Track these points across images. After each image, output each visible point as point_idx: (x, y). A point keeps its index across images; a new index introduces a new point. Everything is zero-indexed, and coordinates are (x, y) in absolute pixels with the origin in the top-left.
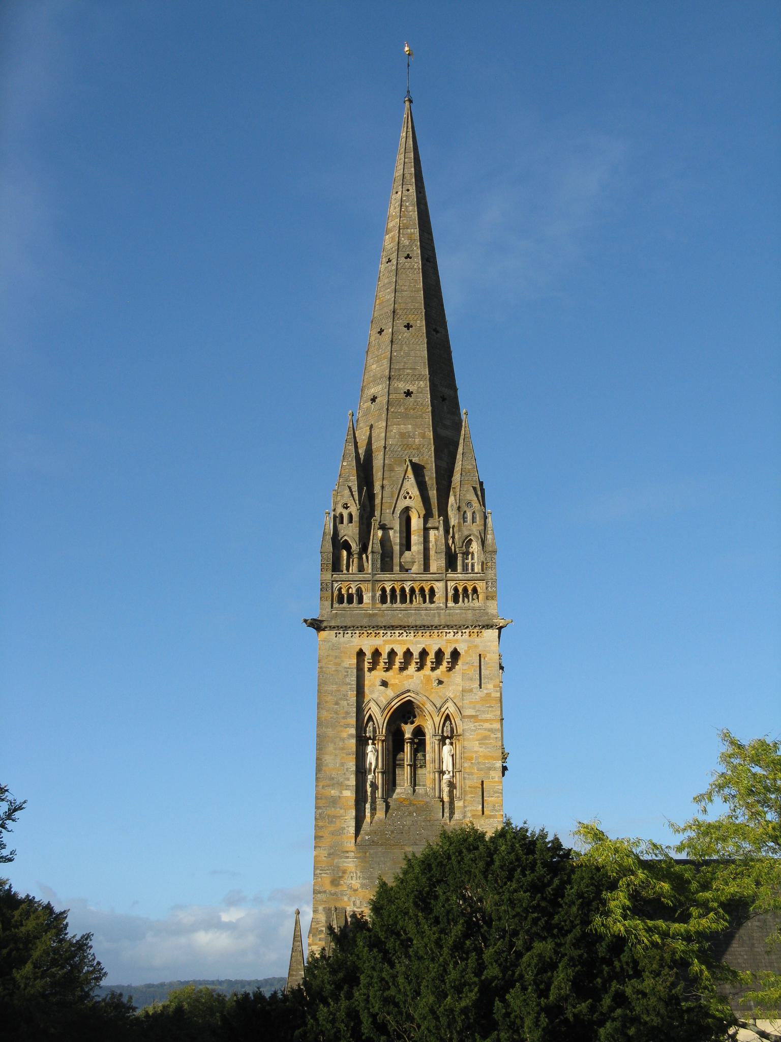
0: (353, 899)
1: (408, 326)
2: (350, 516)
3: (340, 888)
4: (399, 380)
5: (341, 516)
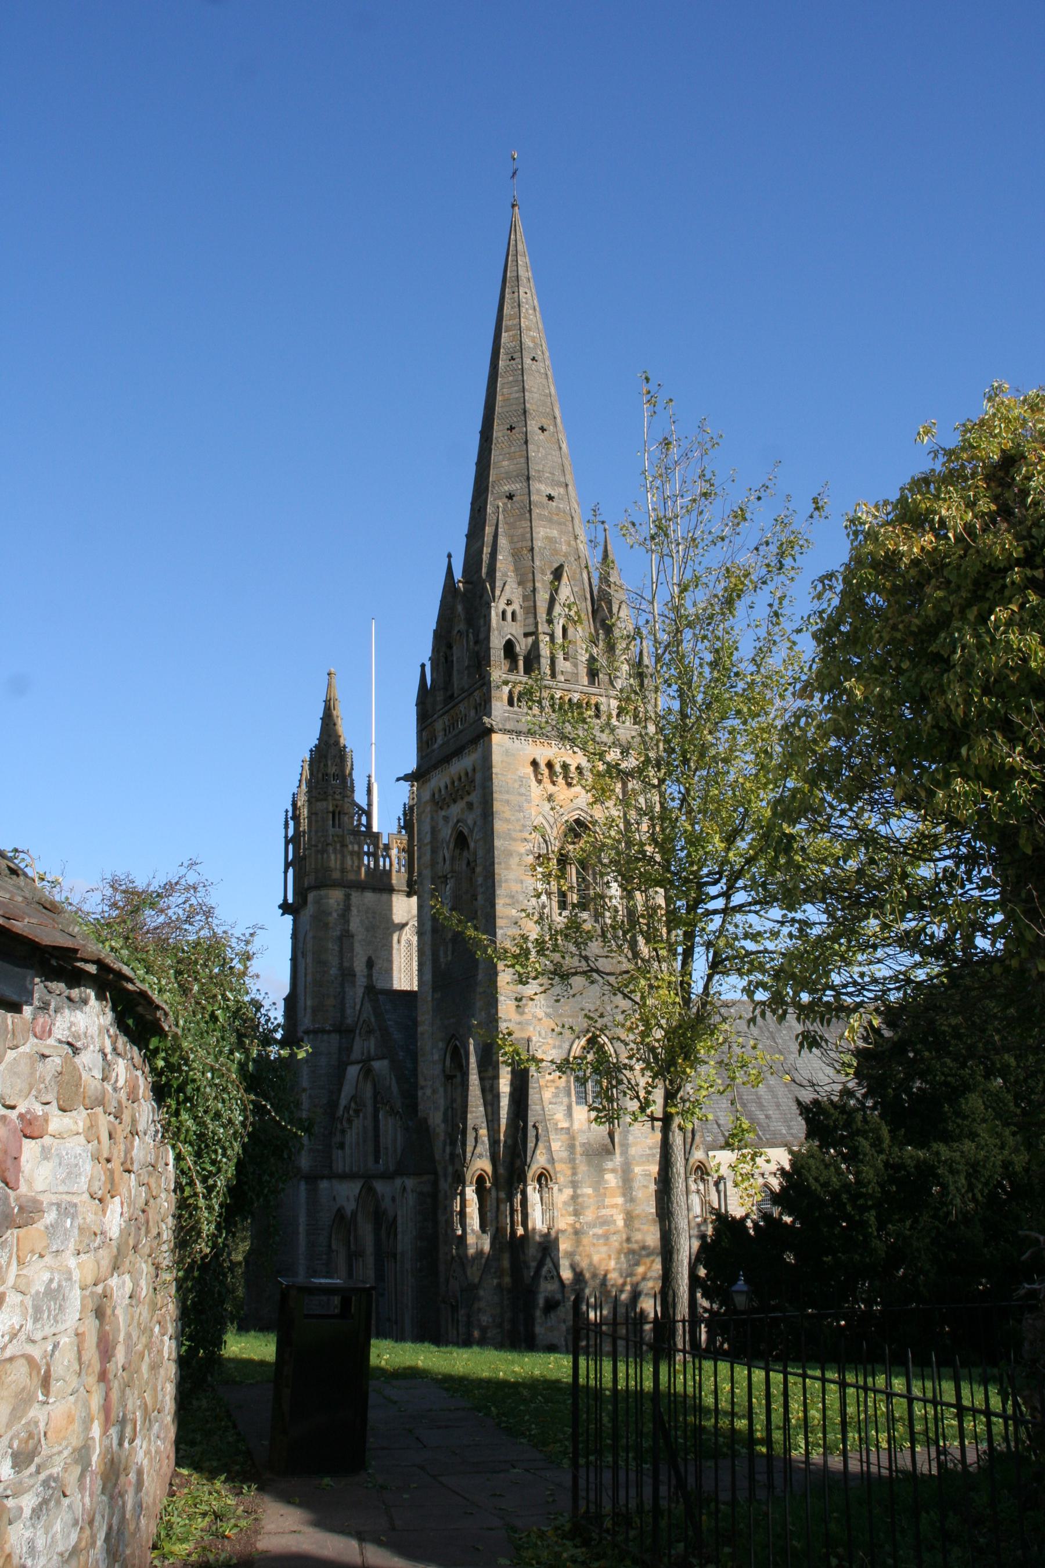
0: (538, 1028)
1: (543, 429)
2: (513, 614)
3: (526, 1017)
4: (540, 481)
5: (504, 613)
